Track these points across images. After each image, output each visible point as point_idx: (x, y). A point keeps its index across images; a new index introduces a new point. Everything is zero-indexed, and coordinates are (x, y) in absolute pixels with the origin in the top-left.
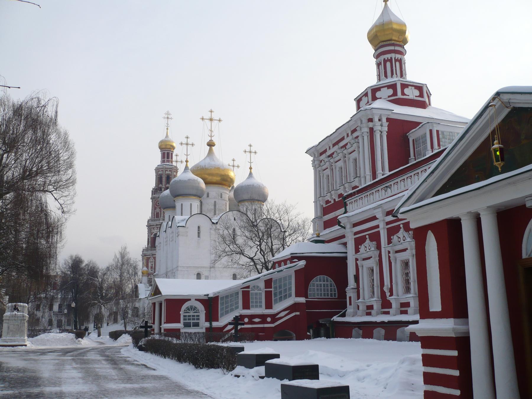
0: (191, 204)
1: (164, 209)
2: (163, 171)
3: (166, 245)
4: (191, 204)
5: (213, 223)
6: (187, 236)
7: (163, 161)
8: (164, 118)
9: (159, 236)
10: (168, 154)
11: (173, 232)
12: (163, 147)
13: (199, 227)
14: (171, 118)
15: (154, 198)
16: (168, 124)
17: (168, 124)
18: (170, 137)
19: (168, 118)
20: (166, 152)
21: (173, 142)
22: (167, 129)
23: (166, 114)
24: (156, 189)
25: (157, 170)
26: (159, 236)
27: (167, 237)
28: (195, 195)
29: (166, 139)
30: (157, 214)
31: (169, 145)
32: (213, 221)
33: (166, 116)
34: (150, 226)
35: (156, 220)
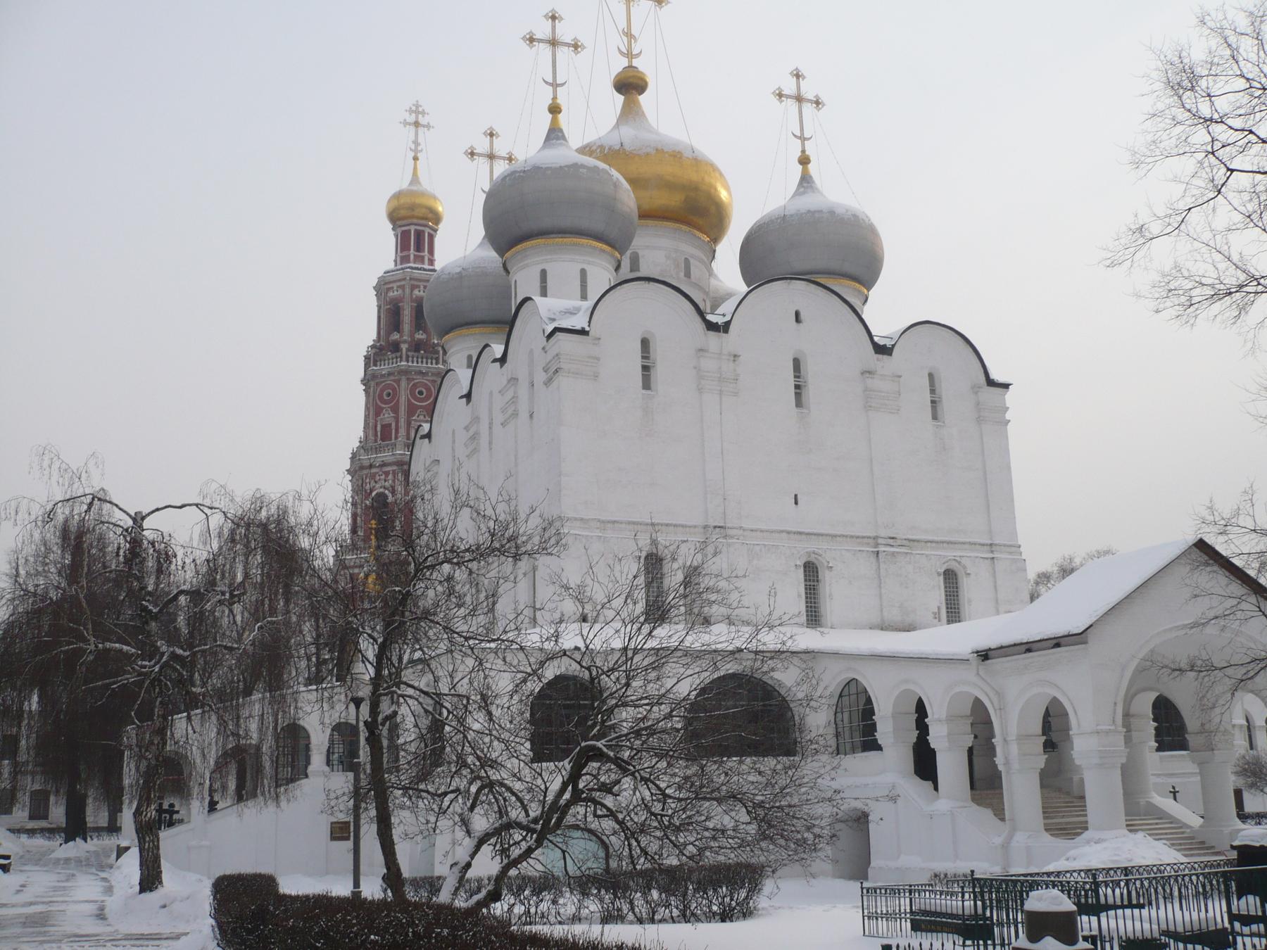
0: (583, 273)
1: (441, 336)
2: (403, 287)
3: (475, 451)
4: (583, 273)
5: (712, 327)
6: (596, 376)
7: (405, 259)
8: (405, 123)
9: (428, 436)
10: (419, 235)
11: (513, 380)
12: (403, 213)
13: (645, 343)
14: (428, 126)
15: (374, 376)
16: (416, 143)
17: (416, 143)
18: (426, 184)
19: (417, 124)
20: (413, 228)
21: (435, 198)
22: (415, 159)
23: (411, 111)
24: (381, 349)
25: (382, 287)
26: (428, 436)
27: (476, 419)
28: (599, 238)
29: (414, 188)
30: (386, 427)
31: (420, 206)
32: (709, 317)
33: (412, 118)
34: (362, 468)
35: (378, 450)
